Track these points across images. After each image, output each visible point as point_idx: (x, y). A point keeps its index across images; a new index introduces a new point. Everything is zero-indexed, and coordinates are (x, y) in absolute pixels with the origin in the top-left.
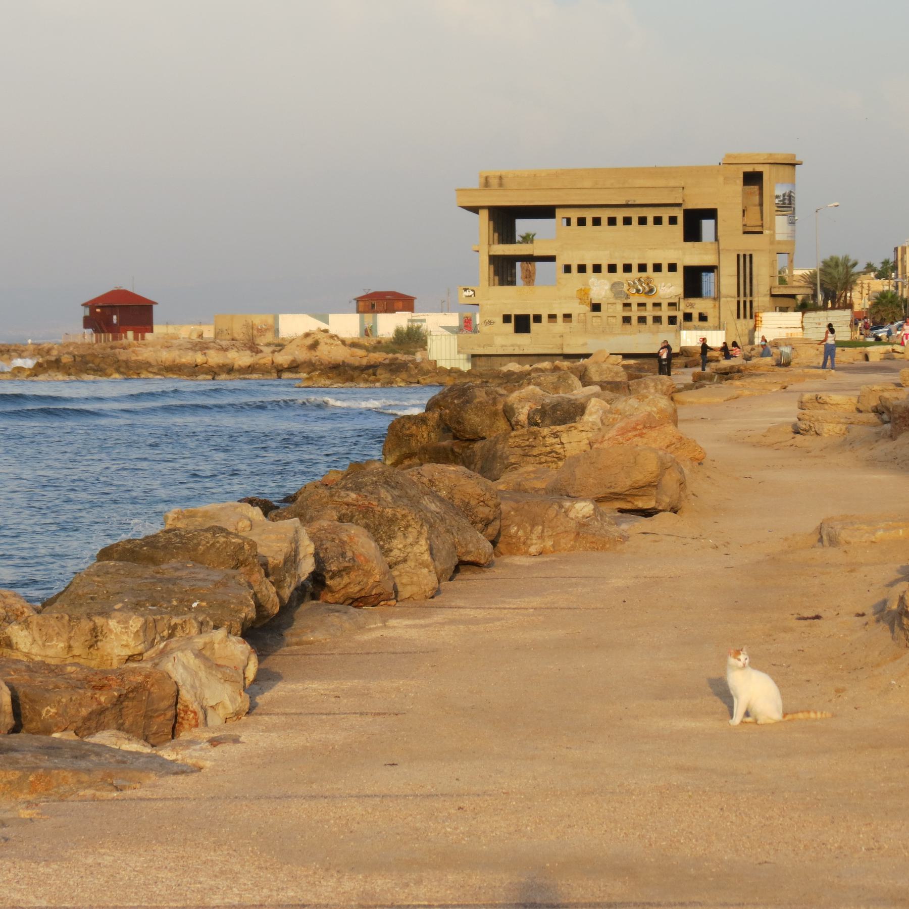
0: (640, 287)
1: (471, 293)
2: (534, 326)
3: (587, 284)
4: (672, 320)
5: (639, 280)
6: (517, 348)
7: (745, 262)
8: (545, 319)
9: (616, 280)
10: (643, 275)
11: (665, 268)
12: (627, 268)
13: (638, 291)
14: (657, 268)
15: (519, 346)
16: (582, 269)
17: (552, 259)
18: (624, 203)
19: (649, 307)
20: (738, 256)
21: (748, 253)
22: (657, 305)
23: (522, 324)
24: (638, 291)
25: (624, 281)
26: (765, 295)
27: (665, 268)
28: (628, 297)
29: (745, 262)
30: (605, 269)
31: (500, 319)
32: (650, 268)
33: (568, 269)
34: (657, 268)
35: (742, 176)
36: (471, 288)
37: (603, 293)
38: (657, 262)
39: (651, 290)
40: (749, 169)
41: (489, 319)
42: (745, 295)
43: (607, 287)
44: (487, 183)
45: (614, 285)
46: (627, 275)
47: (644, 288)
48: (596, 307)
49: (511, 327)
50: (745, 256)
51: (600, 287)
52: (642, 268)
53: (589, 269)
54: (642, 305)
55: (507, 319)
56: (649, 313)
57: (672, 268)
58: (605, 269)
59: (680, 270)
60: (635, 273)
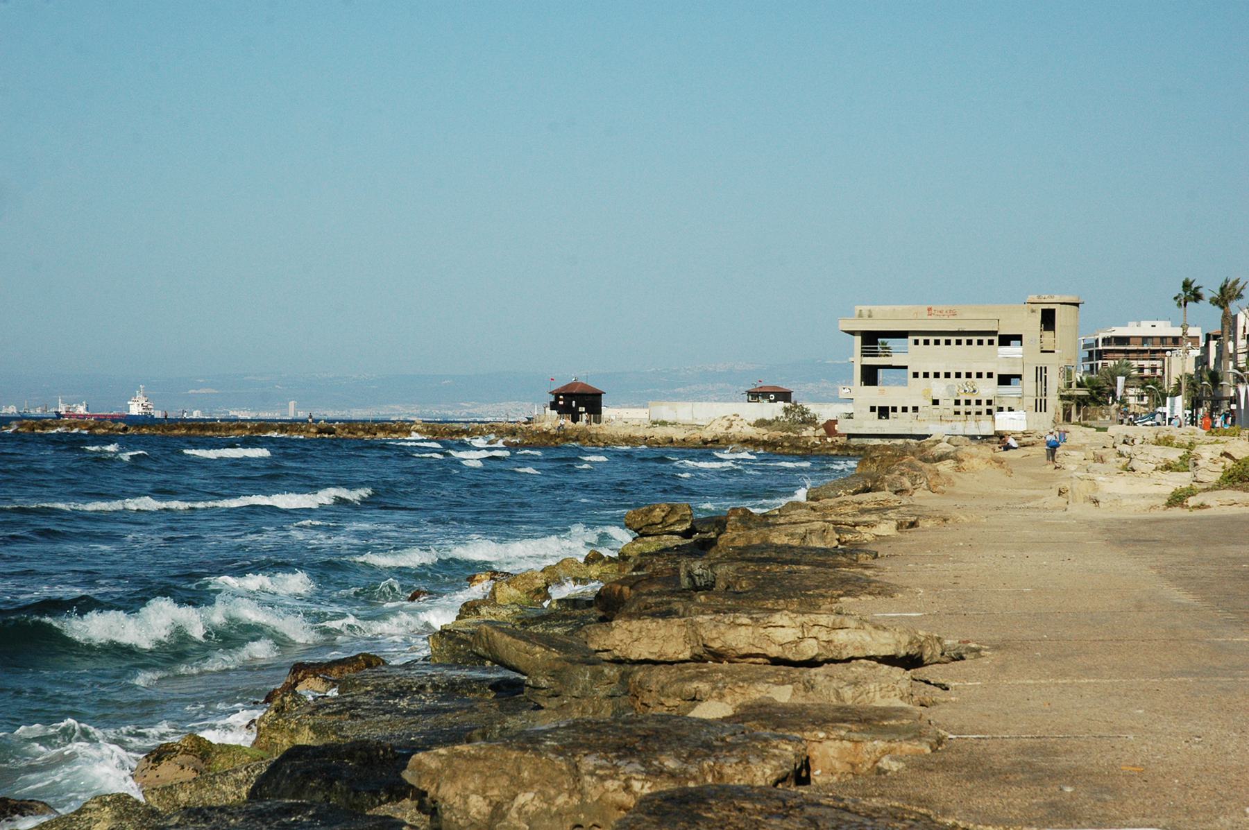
2: (891, 414)
4: (989, 412)
8: (899, 409)
11: (985, 375)
12: (958, 375)
14: (979, 375)
16: (926, 375)
17: (906, 367)
19: (973, 402)
22: (979, 402)
23: (883, 412)
27: (985, 375)
30: (942, 375)
32: (974, 375)
34: (979, 375)
40: (1046, 307)
43: (944, 388)
44: (860, 316)
48: (936, 402)
51: (939, 388)
52: (969, 375)
53: (931, 375)
54: (968, 402)
55: (873, 409)
56: (973, 408)
57: (990, 375)
58: (942, 375)
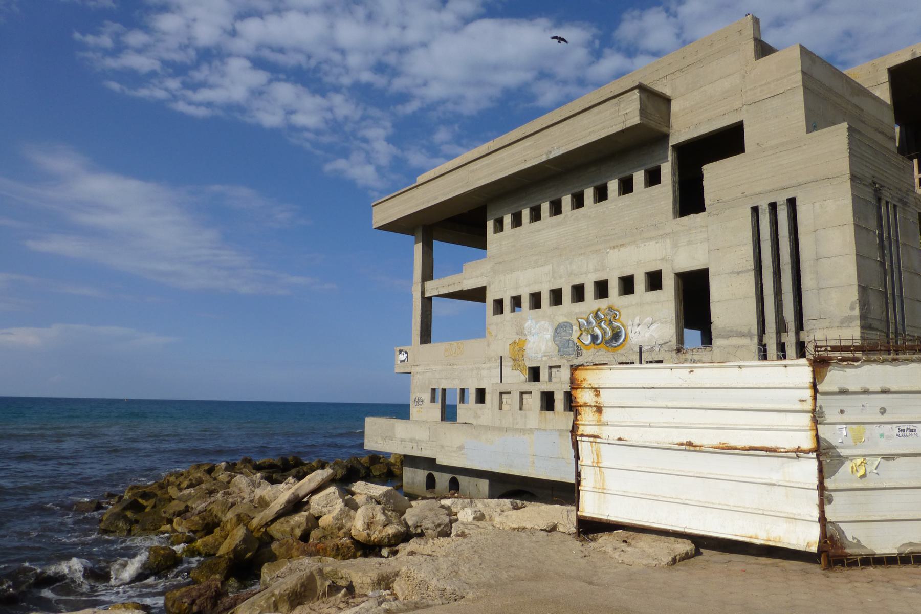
0: (598, 331)
3: (520, 331)
5: (596, 316)
6: (415, 445)
7: (778, 231)
9: (562, 319)
10: (603, 303)
11: (640, 284)
13: (594, 338)
14: (627, 285)
15: (417, 442)
20: (755, 210)
21: (781, 200)
24: (594, 338)
25: (574, 322)
26: (845, 322)
27: (640, 284)
28: (579, 354)
29: (778, 231)
31: (427, 397)
32: (614, 288)
35: (885, 77)
36: (405, 348)
37: (543, 348)
38: (627, 273)
39: (616, 336)
42: (781, 327)
43: (549, 335)
46: (579, 307)
47: (604, 333)
49: (436, 411)
50: (773, 206)
52: (602, 289)
57: (654, 281)
58: (545, 299)
60: (591, 303)
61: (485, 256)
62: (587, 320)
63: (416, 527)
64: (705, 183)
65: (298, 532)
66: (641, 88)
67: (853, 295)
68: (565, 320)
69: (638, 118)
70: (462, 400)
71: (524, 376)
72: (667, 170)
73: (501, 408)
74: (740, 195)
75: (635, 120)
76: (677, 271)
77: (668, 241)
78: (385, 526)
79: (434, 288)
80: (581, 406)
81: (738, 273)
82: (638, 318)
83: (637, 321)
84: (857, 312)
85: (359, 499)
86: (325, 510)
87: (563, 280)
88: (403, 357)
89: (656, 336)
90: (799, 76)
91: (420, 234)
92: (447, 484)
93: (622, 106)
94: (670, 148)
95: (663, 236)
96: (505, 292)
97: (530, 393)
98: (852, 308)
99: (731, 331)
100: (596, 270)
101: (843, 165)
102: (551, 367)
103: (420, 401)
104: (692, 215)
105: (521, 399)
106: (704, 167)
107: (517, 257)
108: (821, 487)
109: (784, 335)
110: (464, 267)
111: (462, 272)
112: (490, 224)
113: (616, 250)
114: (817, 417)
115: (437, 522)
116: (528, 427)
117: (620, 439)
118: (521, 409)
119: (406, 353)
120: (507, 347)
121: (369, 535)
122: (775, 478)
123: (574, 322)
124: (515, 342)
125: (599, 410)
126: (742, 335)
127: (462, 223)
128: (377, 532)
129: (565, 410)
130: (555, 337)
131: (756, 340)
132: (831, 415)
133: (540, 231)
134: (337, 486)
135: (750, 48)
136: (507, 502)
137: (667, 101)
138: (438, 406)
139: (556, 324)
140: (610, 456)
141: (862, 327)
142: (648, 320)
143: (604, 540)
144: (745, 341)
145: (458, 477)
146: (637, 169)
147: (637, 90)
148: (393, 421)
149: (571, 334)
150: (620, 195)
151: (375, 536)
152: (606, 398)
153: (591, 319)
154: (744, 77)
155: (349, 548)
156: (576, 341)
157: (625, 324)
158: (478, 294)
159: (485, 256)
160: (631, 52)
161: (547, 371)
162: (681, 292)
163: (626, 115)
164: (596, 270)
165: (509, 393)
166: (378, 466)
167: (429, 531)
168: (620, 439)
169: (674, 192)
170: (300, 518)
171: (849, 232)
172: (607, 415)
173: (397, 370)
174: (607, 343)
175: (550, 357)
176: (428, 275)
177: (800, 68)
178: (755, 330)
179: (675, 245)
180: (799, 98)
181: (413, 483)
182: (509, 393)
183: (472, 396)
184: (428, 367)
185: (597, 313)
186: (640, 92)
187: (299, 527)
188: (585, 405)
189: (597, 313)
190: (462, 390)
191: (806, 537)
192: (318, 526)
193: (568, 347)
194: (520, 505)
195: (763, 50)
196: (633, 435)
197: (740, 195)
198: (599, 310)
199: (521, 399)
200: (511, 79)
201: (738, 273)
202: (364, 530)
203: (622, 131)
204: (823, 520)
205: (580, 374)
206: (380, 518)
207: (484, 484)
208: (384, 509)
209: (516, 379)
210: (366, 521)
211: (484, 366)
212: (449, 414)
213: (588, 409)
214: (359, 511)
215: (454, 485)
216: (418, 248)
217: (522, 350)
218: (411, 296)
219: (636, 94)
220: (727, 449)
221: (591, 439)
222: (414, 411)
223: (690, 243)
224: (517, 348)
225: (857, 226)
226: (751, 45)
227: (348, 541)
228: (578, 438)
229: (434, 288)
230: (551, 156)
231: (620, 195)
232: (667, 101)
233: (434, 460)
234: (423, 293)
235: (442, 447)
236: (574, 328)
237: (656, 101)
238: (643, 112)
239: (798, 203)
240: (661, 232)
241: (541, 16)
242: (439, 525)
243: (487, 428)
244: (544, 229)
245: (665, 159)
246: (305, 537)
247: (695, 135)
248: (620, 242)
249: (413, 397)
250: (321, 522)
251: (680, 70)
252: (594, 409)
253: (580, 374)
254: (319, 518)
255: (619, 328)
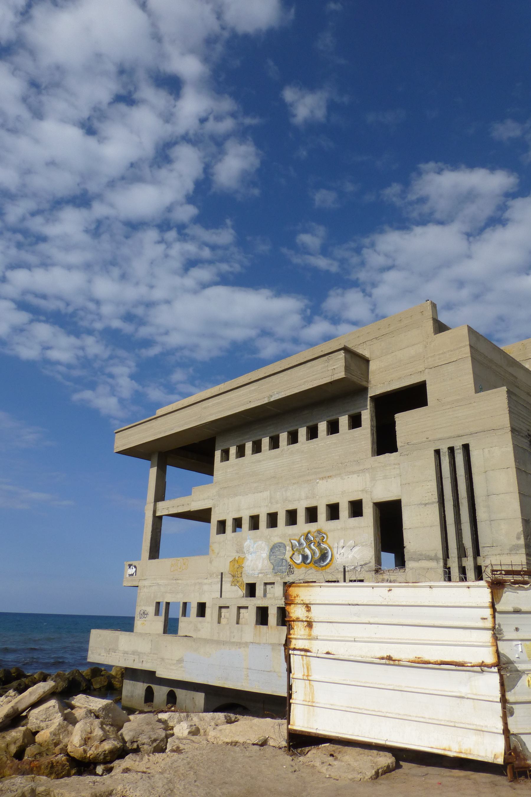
0: (308, 552)
1: (134, 569)
3: (240, 550)
5: (307, 538)
6: (136, 657)
9: (276, 540)
10: (313, 527)
11: (344, 511)
13: (305, 558)
14: (333, 511)
18: (266, 401)
20: (437, 452)
21: (458, 445)
25: (287, 543)
26: (513, 549)
27: (344, 511)
28: (291, 571)
31: (151, 610)
32: (322, 514)
33: (222, 525)
36: (134, 563)
37: (260, 566)
38: (333, 501)
39: (324, 556)
41: (144, 608)
42: (462, 553)
43: (265, 554)
45: (275, 549)
46: (292, 529)
47: (314, 553)
49: (159, 623)
50: (451, 450)
52: (312, 514)
57: (356, 509)
58: (263, 522)
59: (368, 510)
60: (302, 526)
61: (211, 482)
62: (300, 544)
63: (133, 742)
64: (397, 428)
65: (13, 749)
66: (346, 350)
67: (518, 527)
68: (280, 540)
69: (344, 373)
70: (184, 614)
71: (242, 592)
72: (366, 416)
73: (219, 622)
74: (425, 439)
75: (341, 374)
76: (375, 501)
77: (367, 475)
78: (102, 741)
79: (165, 508)
80: (294, 621)
81: (426, 504)
82: (342, 541)
83: (341, 544)
84: (522, 541)
85: (78, 713)
86: (43, 725)
87: (279, 505)
88: (132, 571)
89: (358, 557)
90: (468, 349)
91: (155, 459)
92: (165, 697)
93: (331, 362)
94: (369, 399)
95: (363, 471)
96: (228, 514)
97: (247, 608)
98: (518, 538)
99: (421, 555)
100: (307, 498)
101: (505, 420)
102: (266, 584)
103: (144, 614)
104: (387, 454)
105: (239, 614)
106: (396, 416)
107: (240, 483)
108: (504, 700)
109: (464, 559)
110: (193, 490)
111: (191, 495)
112: (218, 454)
113: (324, 481)
114: (497, 634)
115: (154, 737)
116: (244, 640)
117: (328, 653)
118: (238, 623)
119: (135, 567)
120: (228, 564)
121: (85, 751)
122: (464, 691)
123: (287, 543)
124: (235, 560)
125: (310, 624)
126: (430, 558)
127: (194, 452)
128: (93, 749)
129: (278, 625)
130: (270, 556)
131: (441, 563)
132: (508, 633)
133: (260, 461)
134: (58, 700)
135: (430, 325)
136: (221, 716)
137: (367, 361)
138: (162, 618)
139: (272, 544)
140: (320, 669)
141: (527, 555)
142: (351, 543)
143: (315, 755)
144: (433, 564)
145: (175, 690)
146: (342, 413)
147: (342, 352)
148: (118, 633)
149: (285, 554)
150: (328, 434)
151: (91, 752)
152: (316, 613)
153: (302, 541)
154: (426, 347)
155: (64, 765)
156: (289, 560)
157: (331, 545)
158: (204, 515)
159: (211, 482)
160: (335, 320)
161: (262, 587)
162: (378, 519)
163: (334, 370)
164: (307, 498)
165: (228, 607)
166: (98, 679)
167: (145, 747)
168: (328, 653)
169: (372, 434)
170: (16, 734)
171: (512, 474)
172: (317, 629)
173: (125, 584)
174: (315, 562)
175: (266, 574)
176: (160, 496)
177: (468, 343)
178: (440, 554)
179: (373, 479)
180: (468, 366)
181: (132, 696)
182: (228, 607)
183: (193, 610)
184: (154, 581)
185: (307, 536)
186: (345, 353)
187: (15, 743)
188: (298, 620)
189: (307, 536)
190: (185, 604)
191: (493, 750)
192: (34, 742)
193: (282, 566)
194: (233, 719)
195: (440, 327)
196: (340, 650)
197: (425, 439)
198: (309, 533)
199: (239, 614)
200: (239, 334)
201: (426, 504)
202: (80, 746)
203: (331, 383)
204: (506, 732)
205: (293, 591)
206: (98, 733)
207: (200, 698)
208: (102, 724)
209: (235, 594)
210: (84, 736)
211: (206, 581)
212: (171, 627)
213: (300, 623)
214: (78, 725)
215: (172, 698)
216: (153, 472)
217: (241, 567)
218: (143, 515)
219: (342, 354)
220: (422, 663)
221: (303, 653)
222: (138, 624)
223: (385, 477)
224: (236, 566)
225: (518, 469)
226: (431, 323)
227: (64, 758)
228: (291, 652)
229: (165, 508)
230: (272, 399)
231: (328, 434)
232: (367, 361)
233: (154, 673)
234: (155, 512)
235: (163, 659)
236: (288, 548)
237: (357, 361)
238: (347, 368)
239: (471, 448)
240: (361, 467)
241: (265, 288)
242: (155, 740)
243: (206, 641)
244: (264, 460)
245: (365, 407)
246: (19, 755)
247: (389, 389)
248: (328, 474)
249: (138, 610)
250: (38, 738)
251: (376, 338)
252: (306, 624)
253: (293, 591)
254: (35, 733)
255: (326, 549)
